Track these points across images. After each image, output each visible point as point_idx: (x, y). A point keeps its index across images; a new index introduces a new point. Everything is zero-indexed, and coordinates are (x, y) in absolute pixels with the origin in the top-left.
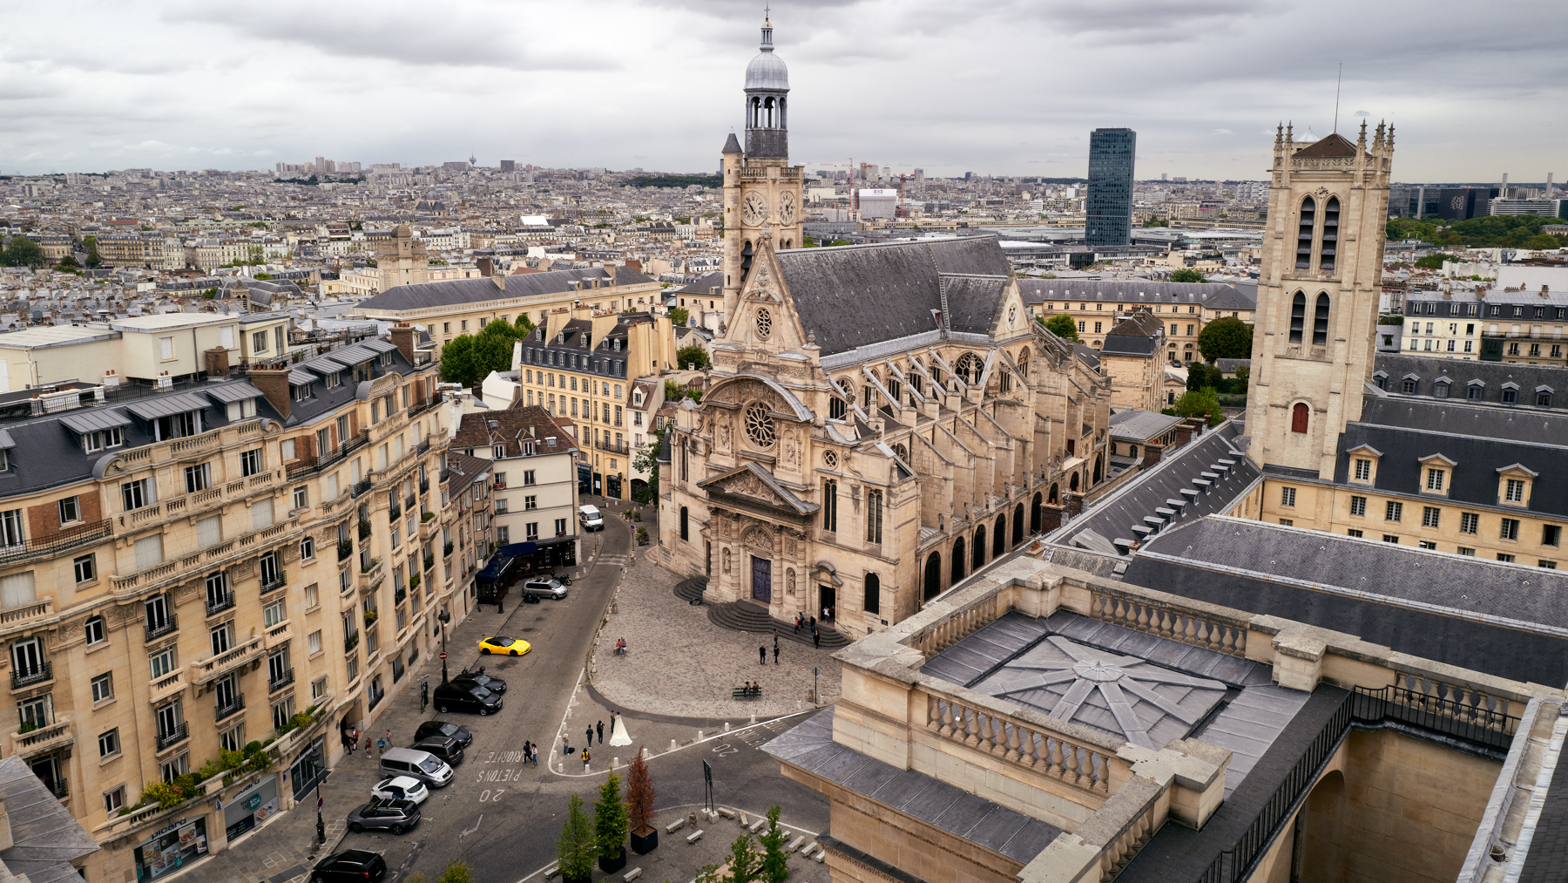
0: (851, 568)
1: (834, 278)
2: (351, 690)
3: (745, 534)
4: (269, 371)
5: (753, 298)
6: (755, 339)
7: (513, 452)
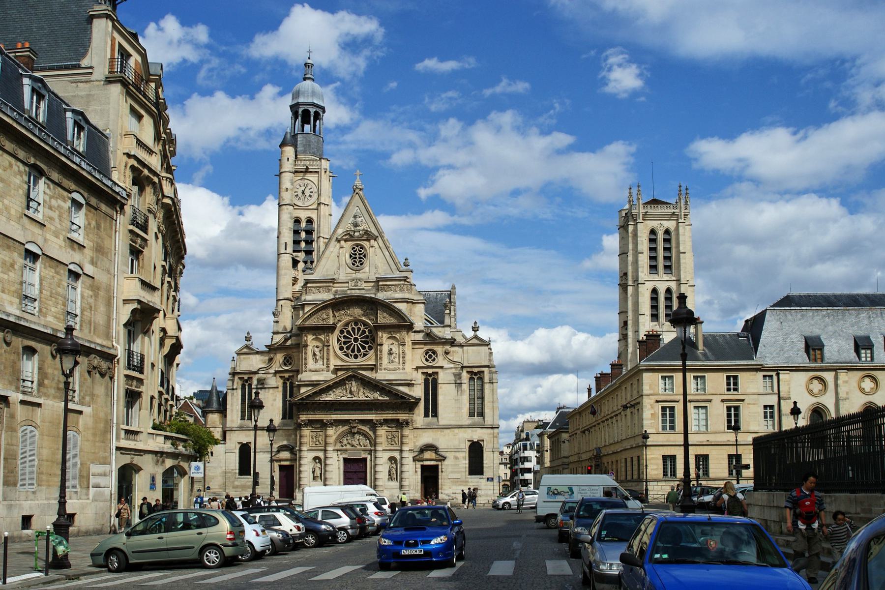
0: (453, 445)
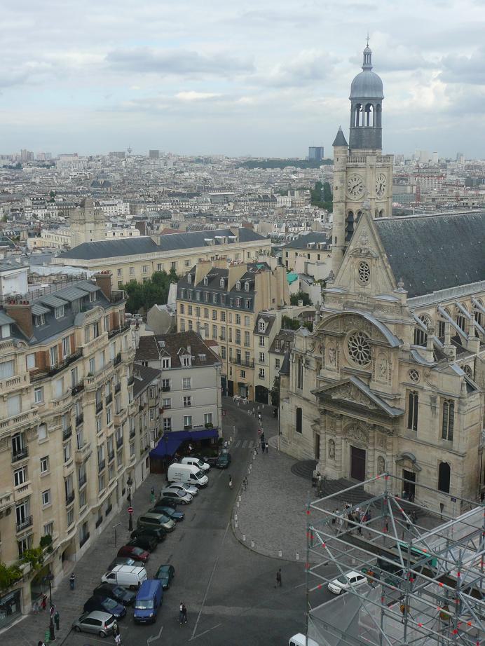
0: (428, 460)
1: (417, 239)
2: (69, 532)
3: (346, 430)
4: (19, 305)
5: (357, 253)
6: (357, 285)
7: (176, 364)
